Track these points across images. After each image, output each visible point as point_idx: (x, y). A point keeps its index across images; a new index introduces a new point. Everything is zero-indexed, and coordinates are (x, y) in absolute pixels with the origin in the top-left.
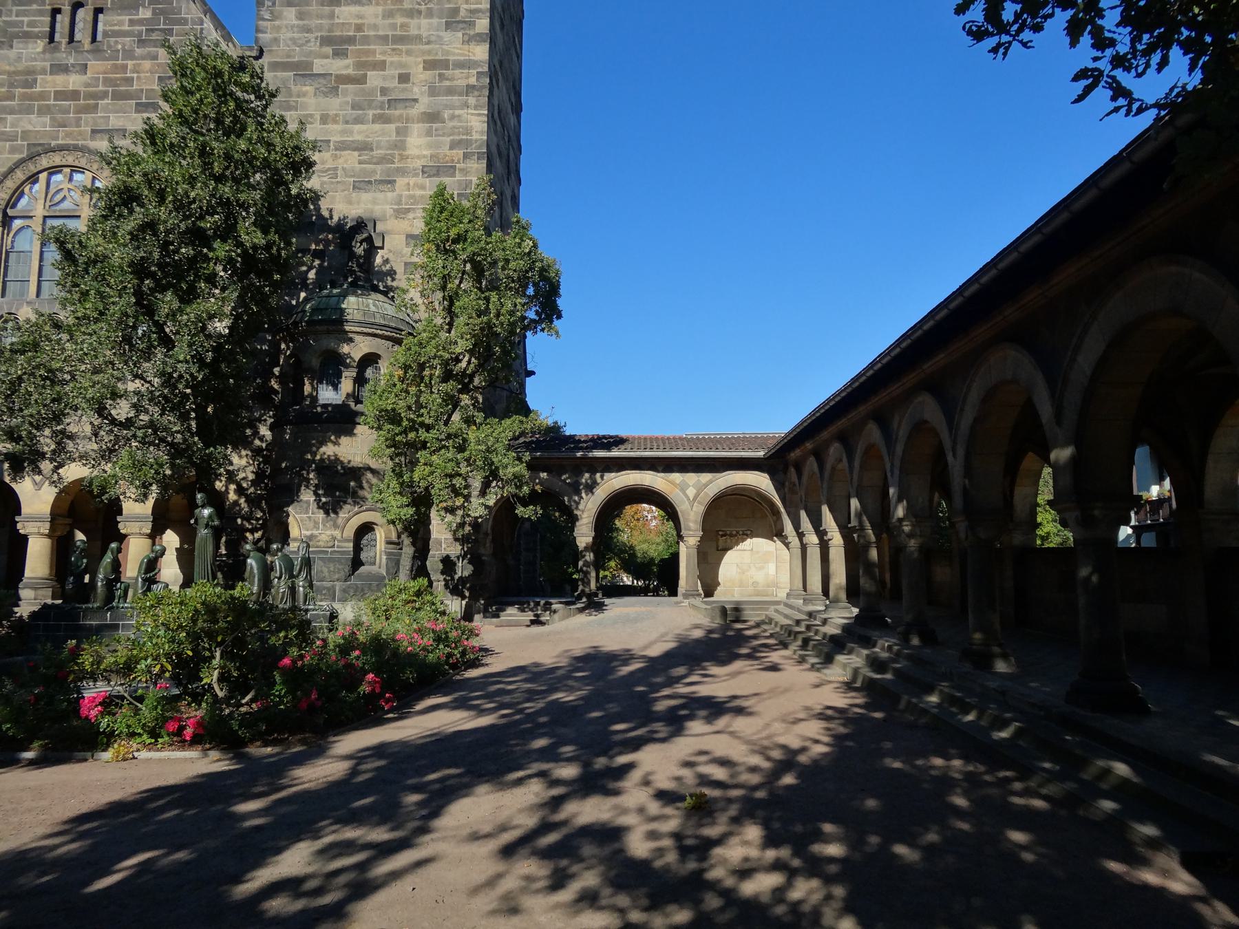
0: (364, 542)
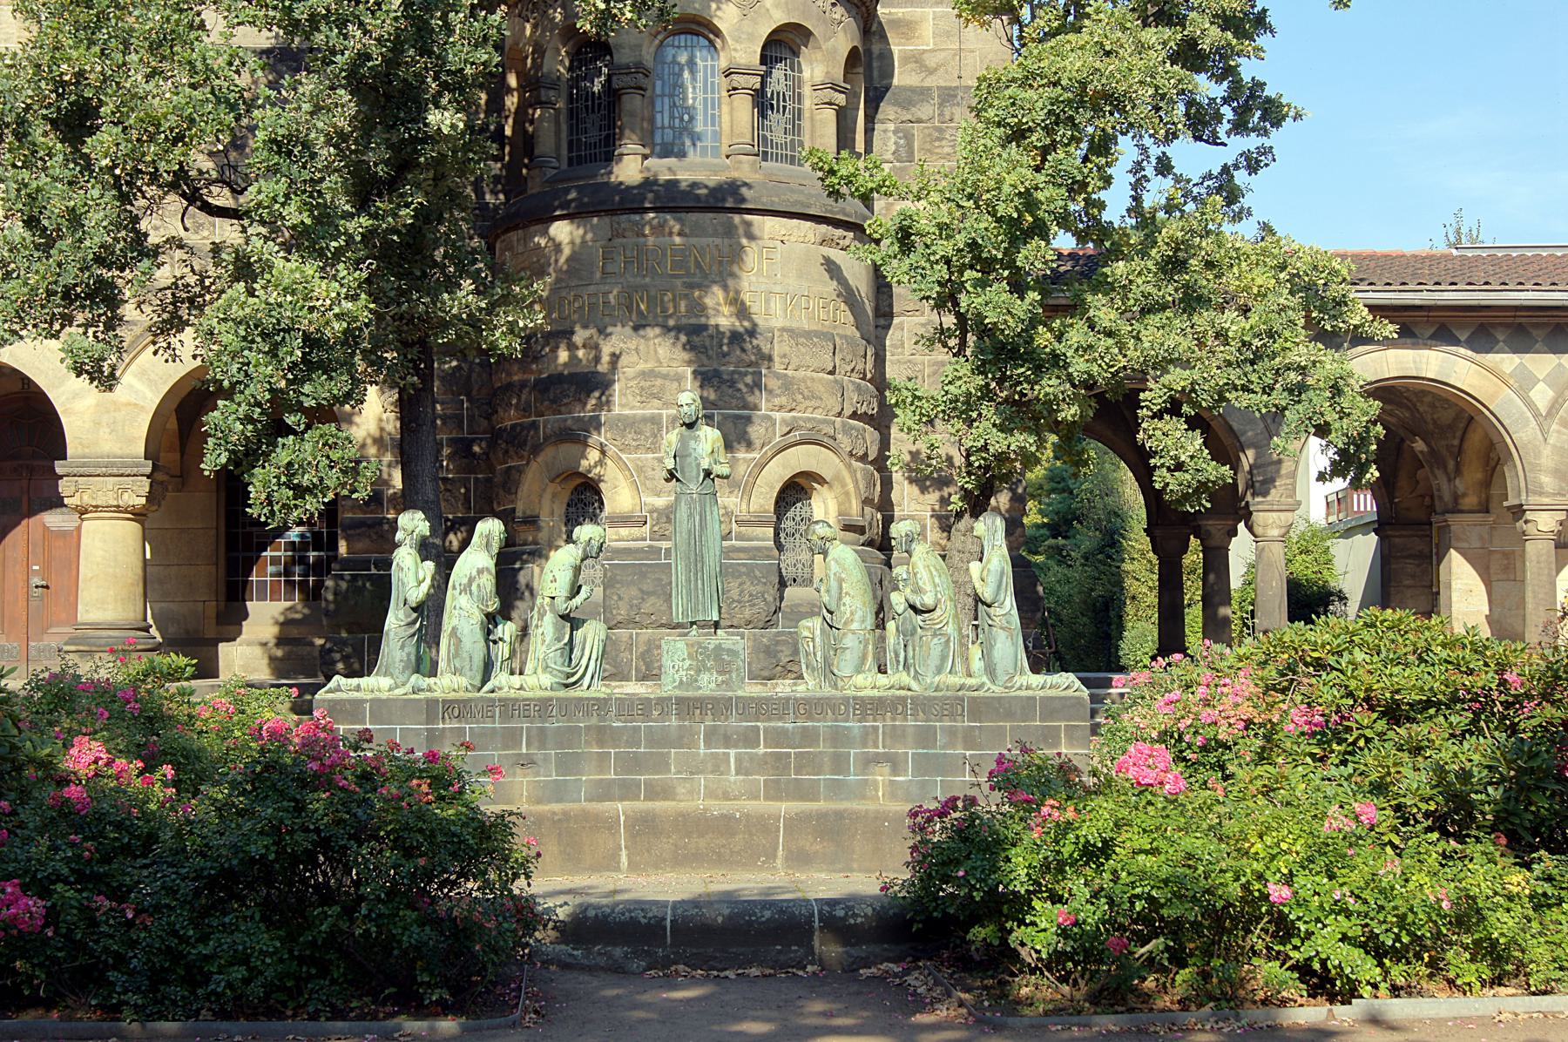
0: (787, 524)
